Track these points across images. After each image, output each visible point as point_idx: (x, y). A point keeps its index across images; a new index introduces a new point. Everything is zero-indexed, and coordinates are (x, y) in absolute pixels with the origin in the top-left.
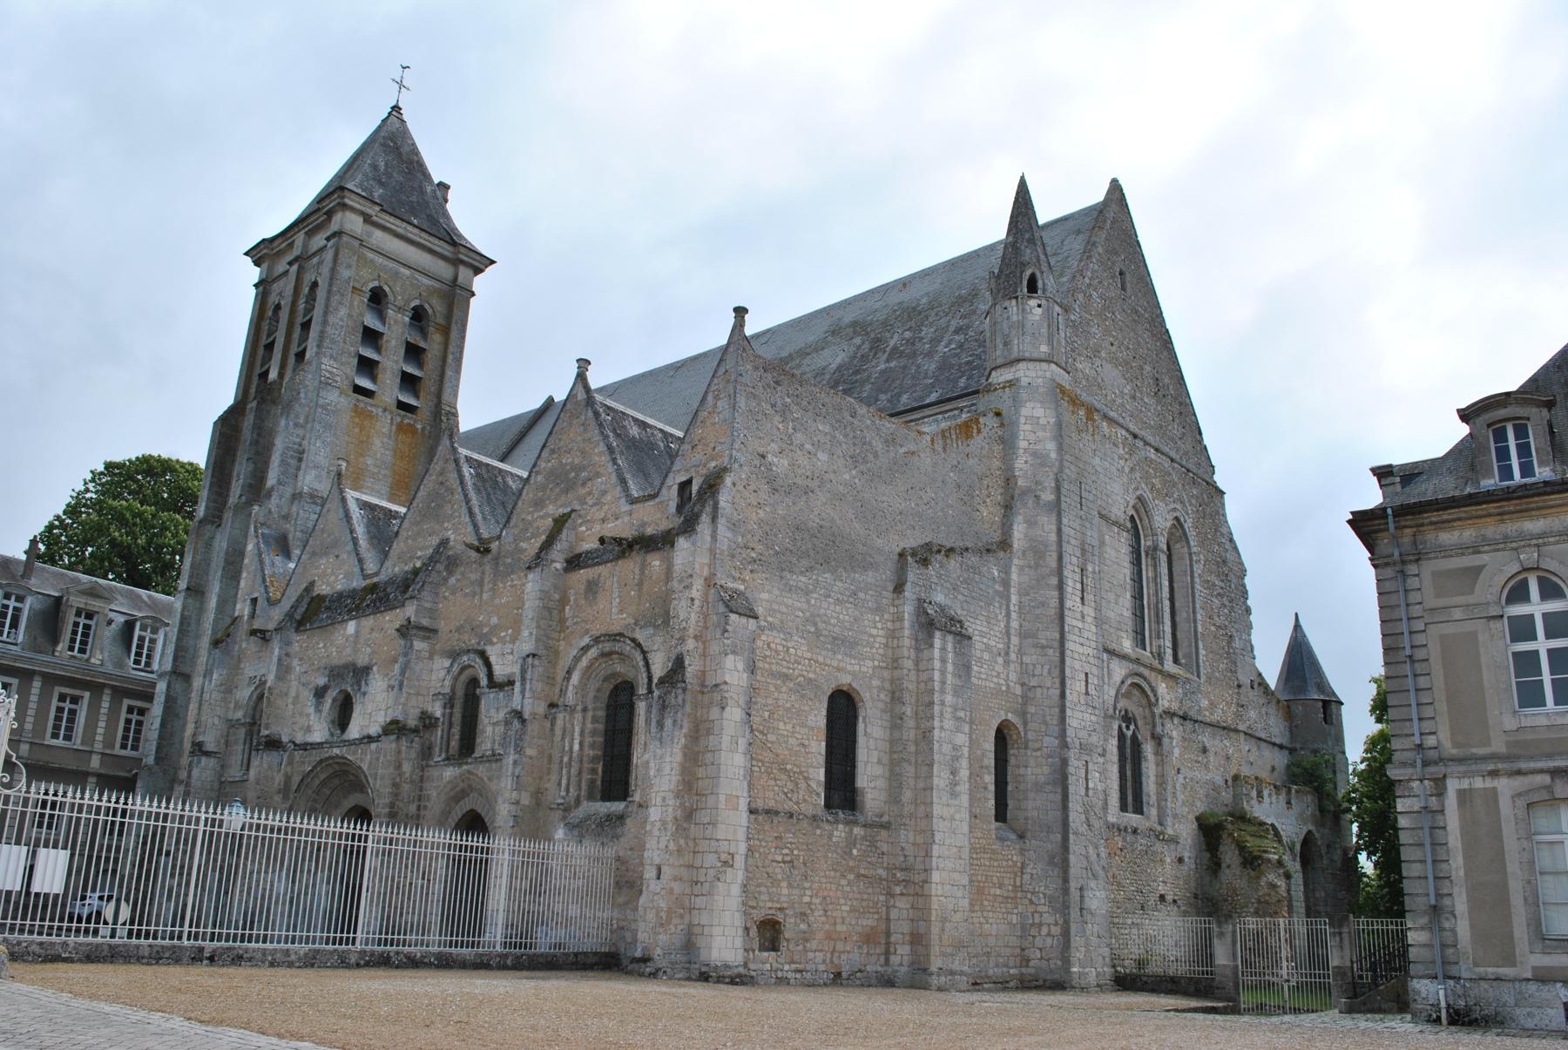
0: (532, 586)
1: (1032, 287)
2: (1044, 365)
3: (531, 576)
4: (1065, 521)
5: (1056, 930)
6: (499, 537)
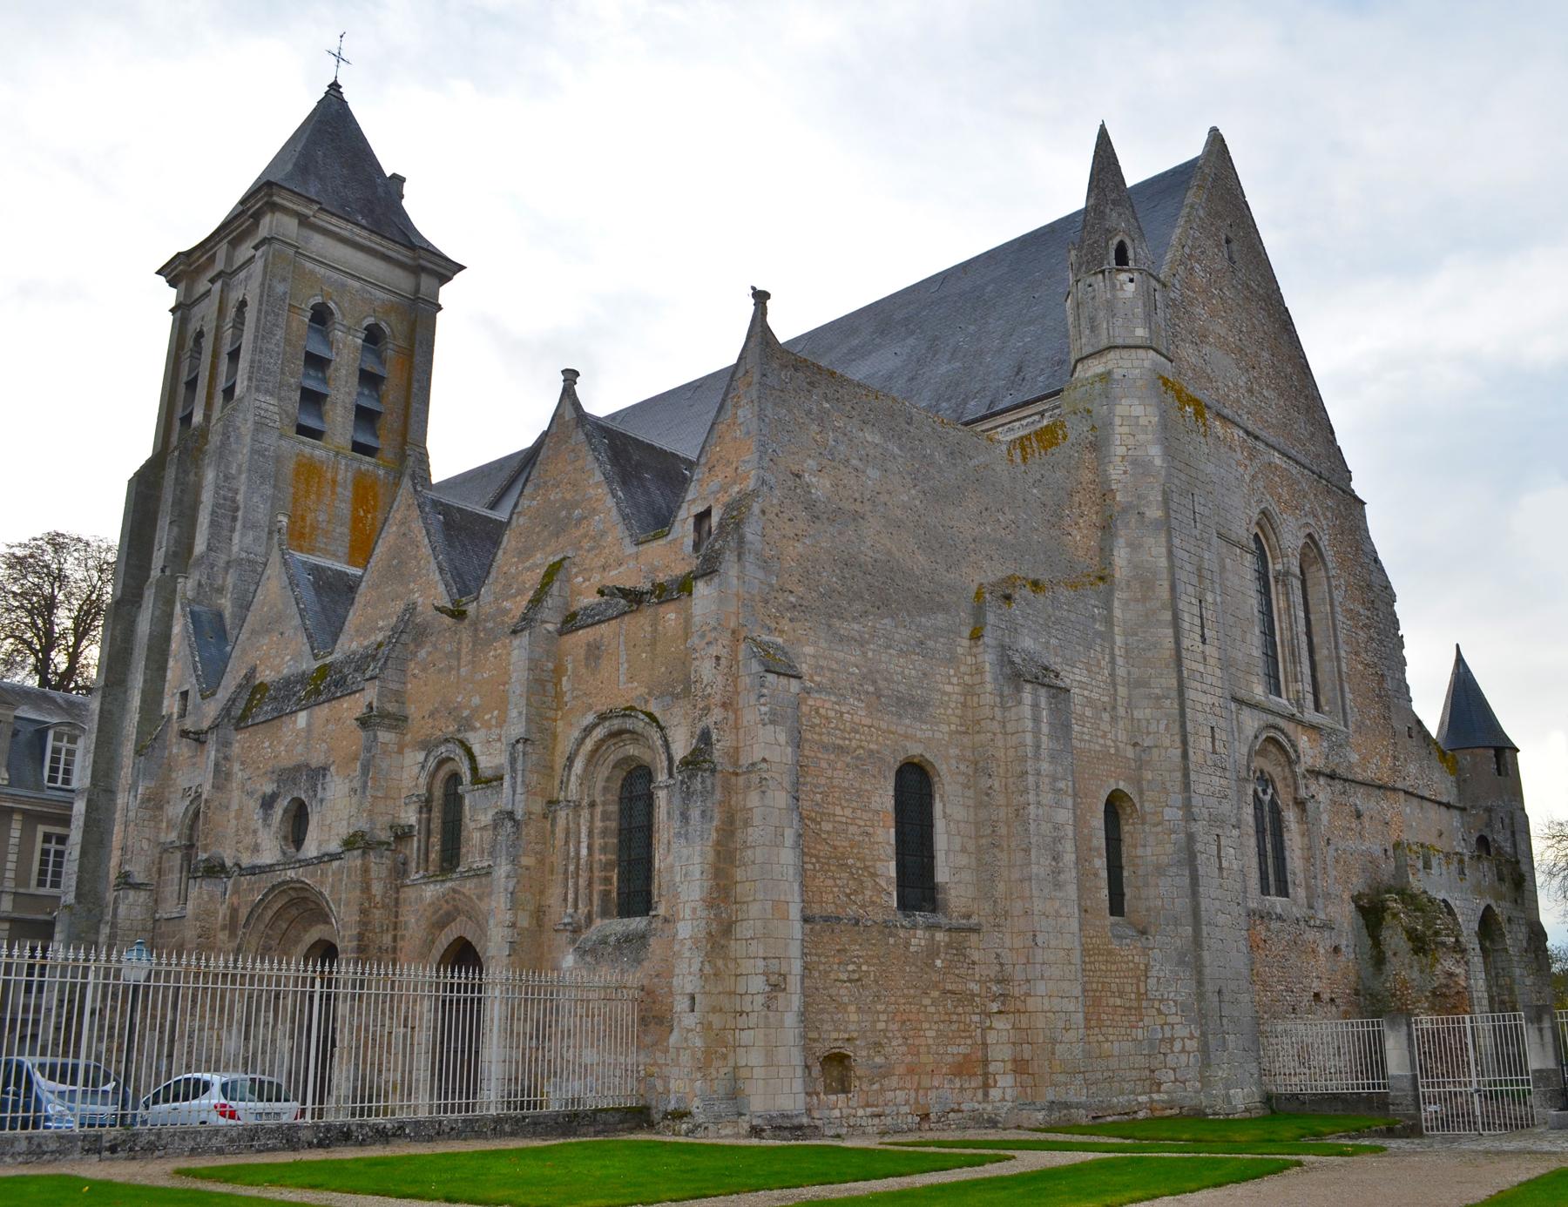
0: (518, 653)
1: (1122, 257)
2: (1141, 353)
3: (516, 642)
4: (1177, 542)
5: (1192, 1045)
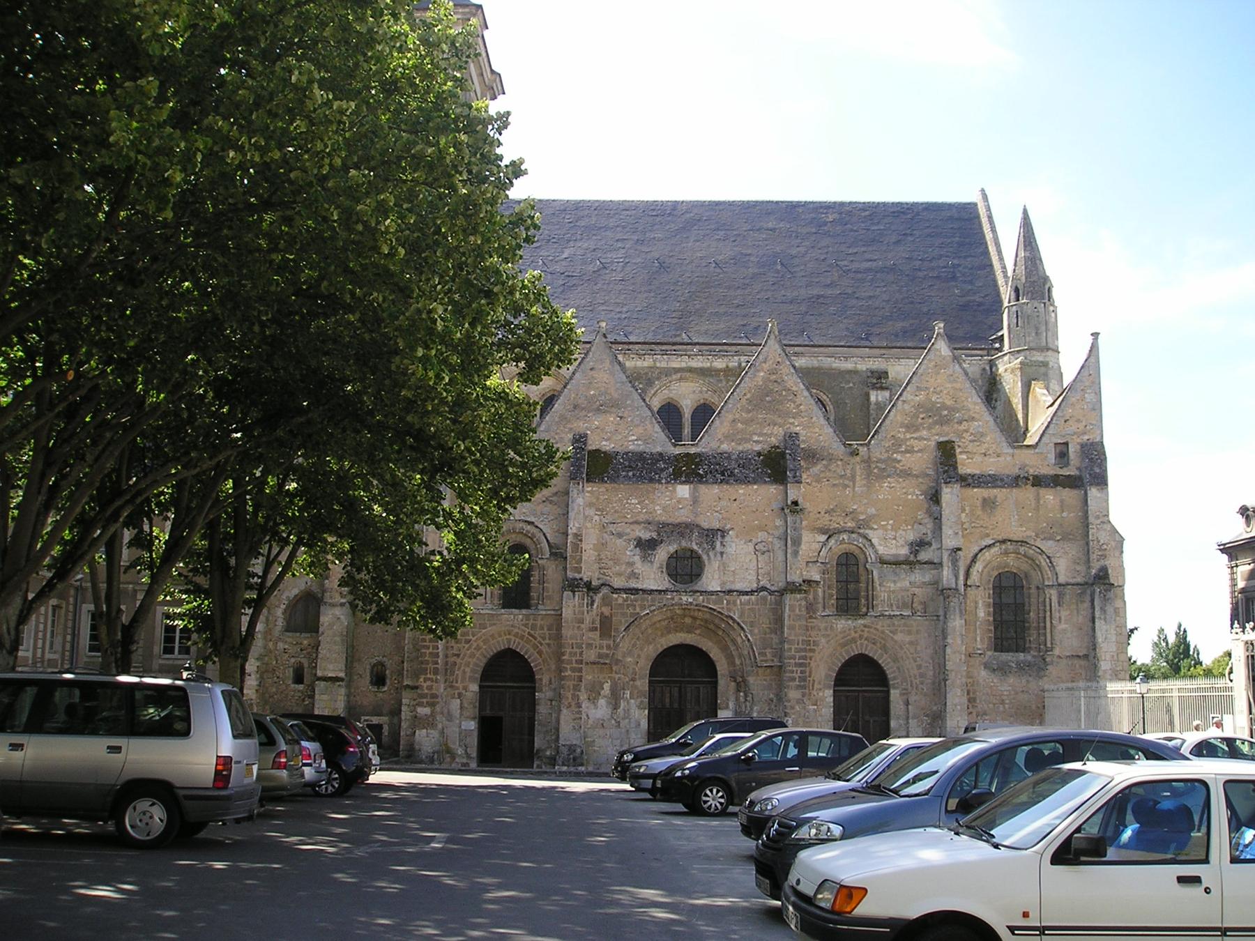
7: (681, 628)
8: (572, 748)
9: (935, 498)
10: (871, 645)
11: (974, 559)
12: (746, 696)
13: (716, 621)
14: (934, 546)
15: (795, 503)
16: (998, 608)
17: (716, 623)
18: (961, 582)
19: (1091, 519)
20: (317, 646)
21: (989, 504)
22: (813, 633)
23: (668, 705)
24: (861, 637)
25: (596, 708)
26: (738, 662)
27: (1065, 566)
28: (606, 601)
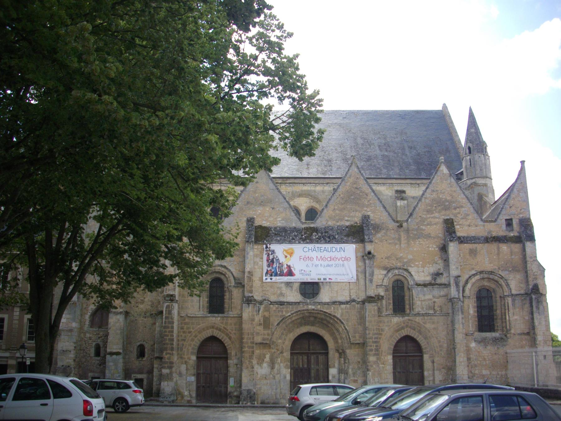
6: (407, 221)
7: (306, 324)
8: (249, 391)
9: (444, 249)
10: (412, 331)
11: (467, 282)
12: (345, 360)
13: (328, 319)
14: (445, 275)
15: (369, 253)
16: (480, 308)
17: (326, 319)
18: (461, 294)
19: (528, 259)
20: (107, 335)
21: (473, 252)
22: (381, 325)
23: (301, 366)
24: (407, 326)
25: (262, 368)
26: (340, 341)
27: (515, 284)
28: (267, 309)
